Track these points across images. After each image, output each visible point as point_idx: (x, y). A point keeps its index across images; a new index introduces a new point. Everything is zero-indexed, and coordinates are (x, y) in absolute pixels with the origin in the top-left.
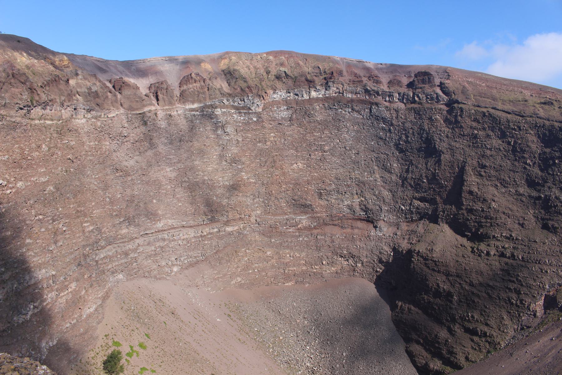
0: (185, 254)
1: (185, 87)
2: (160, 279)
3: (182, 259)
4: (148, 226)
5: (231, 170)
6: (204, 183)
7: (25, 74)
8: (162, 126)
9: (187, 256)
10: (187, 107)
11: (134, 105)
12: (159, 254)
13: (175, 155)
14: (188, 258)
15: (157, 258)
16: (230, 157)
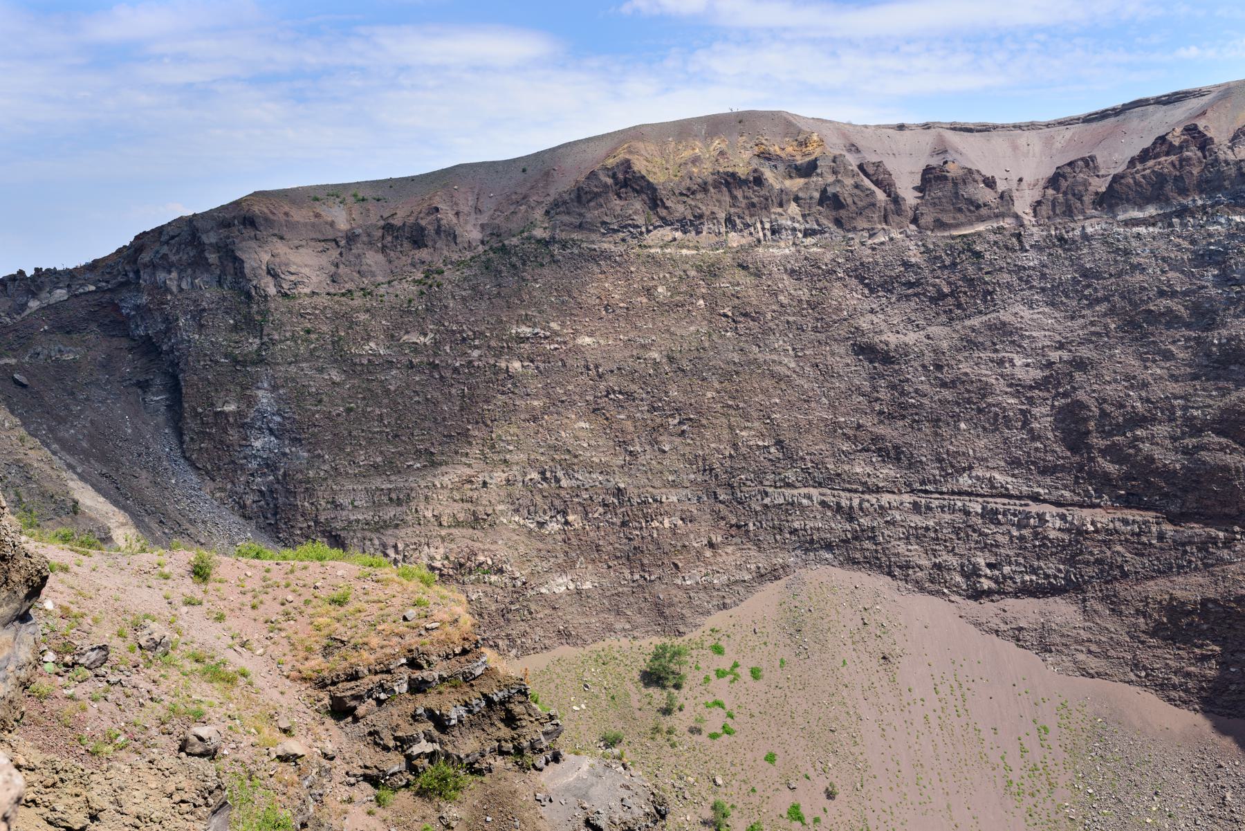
0: (1022, 561)
1: (1139, 167)
2: (930, 593)
3: (1007, 569)
4: (934, 476)
5: (1221, 384)
6: (1122, 406)
7: (643, 177)
8: (1031, 264)
9: (1025, 567)
10: (1121, 217)
11: (946, 218)
12: (945, 541)
13: (1054, 330)
14: (1026, 572)
15: (937, 547)
16: (1224, 345)
